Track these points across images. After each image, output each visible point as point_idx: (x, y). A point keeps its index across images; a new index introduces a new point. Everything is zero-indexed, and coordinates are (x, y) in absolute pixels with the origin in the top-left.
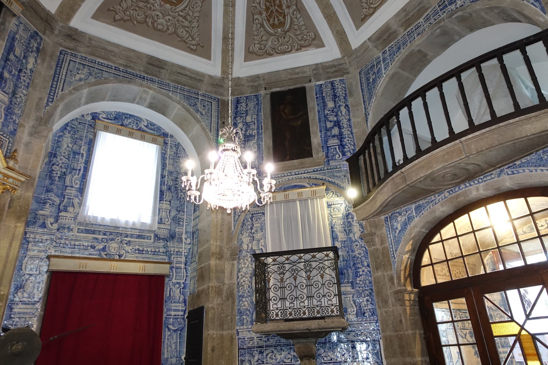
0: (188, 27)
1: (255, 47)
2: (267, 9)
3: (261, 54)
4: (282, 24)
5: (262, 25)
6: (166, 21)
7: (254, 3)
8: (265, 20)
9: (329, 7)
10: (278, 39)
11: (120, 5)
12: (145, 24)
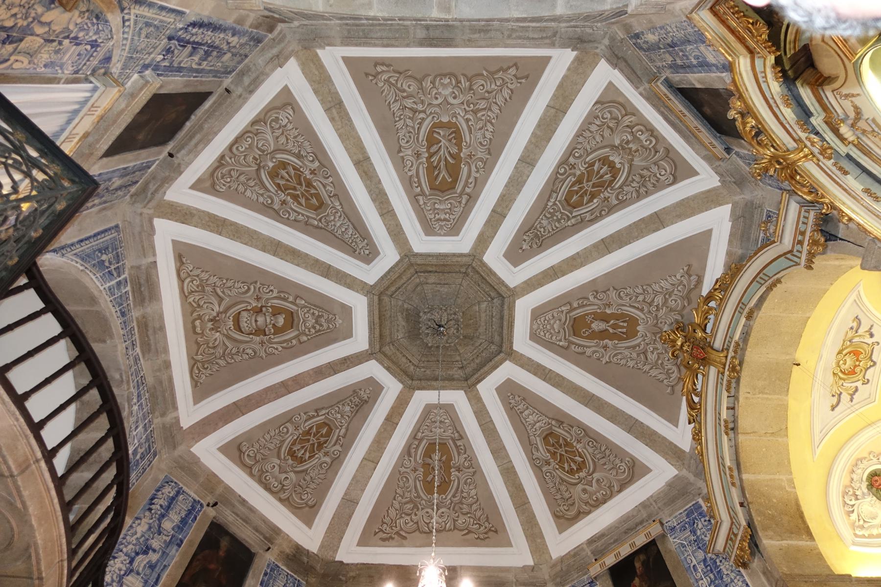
0: (404, 98)
1: (287, 117)
2: (309, 184)
3: (269, 114)
4: (274, 175)
5: (299, 156)
6: (440, 94)
7: (332, 182)
8: (301, 167)
9: (234, 235)
10: (263, 151)
11: (511, 90)
12: (469, 76)
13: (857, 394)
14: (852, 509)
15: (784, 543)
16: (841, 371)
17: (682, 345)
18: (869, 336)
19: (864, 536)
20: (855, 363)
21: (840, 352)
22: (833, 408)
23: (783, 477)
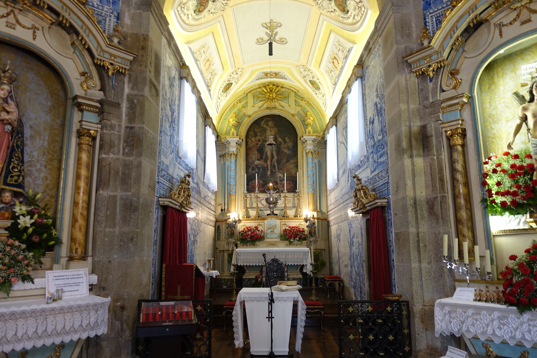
19: (178, 11)
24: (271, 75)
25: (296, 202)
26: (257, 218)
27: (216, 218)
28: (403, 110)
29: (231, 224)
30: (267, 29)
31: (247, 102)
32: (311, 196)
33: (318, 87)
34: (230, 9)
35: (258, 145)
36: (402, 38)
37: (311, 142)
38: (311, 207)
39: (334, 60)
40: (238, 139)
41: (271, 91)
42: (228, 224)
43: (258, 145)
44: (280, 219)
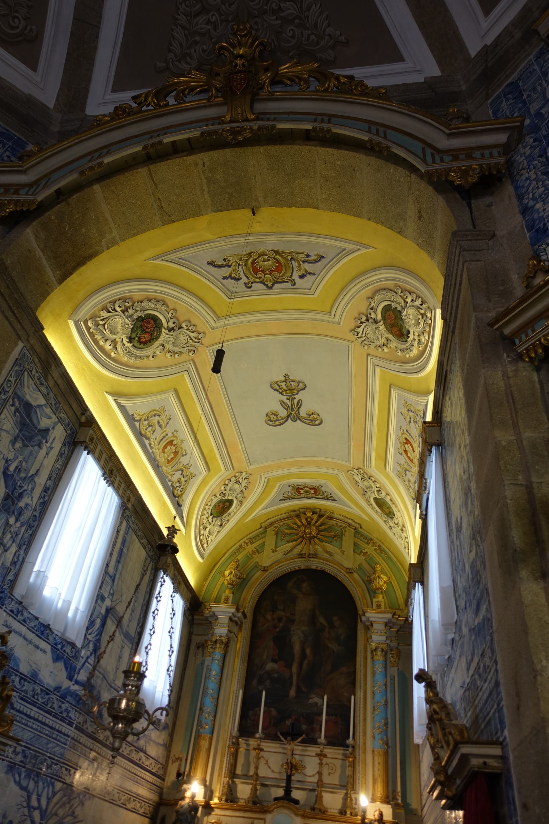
13: (233, 281)
14: (110, 309)
15: (39, 253)
16: (256, 259)
17: (241, 56)
18: (301, 274)
19: (88, 329)
20: (267, 270)
21: (276, 252)
22: (210, 263)
23: (115, 233)
24: (307, 492)
25: (349, 771)
26: (250, 804)
27: (161, 795)
28: (504, 443)
29: (183, 814)
30: (281, 393)
31: (263, 544)
32: (379, 759)
33: (390, 512)
34: (207, 350)
35: (278, 630)
36: (490, 301)
37: (382, 627)
38: (380, 791)
39: (406, 446)
40: (233, 610)
41: (309, 523)
42: (177, 812)
43: (278, 630)
44: (304, 816)
